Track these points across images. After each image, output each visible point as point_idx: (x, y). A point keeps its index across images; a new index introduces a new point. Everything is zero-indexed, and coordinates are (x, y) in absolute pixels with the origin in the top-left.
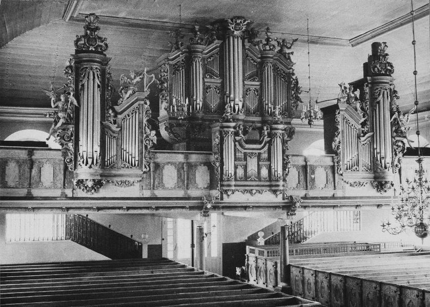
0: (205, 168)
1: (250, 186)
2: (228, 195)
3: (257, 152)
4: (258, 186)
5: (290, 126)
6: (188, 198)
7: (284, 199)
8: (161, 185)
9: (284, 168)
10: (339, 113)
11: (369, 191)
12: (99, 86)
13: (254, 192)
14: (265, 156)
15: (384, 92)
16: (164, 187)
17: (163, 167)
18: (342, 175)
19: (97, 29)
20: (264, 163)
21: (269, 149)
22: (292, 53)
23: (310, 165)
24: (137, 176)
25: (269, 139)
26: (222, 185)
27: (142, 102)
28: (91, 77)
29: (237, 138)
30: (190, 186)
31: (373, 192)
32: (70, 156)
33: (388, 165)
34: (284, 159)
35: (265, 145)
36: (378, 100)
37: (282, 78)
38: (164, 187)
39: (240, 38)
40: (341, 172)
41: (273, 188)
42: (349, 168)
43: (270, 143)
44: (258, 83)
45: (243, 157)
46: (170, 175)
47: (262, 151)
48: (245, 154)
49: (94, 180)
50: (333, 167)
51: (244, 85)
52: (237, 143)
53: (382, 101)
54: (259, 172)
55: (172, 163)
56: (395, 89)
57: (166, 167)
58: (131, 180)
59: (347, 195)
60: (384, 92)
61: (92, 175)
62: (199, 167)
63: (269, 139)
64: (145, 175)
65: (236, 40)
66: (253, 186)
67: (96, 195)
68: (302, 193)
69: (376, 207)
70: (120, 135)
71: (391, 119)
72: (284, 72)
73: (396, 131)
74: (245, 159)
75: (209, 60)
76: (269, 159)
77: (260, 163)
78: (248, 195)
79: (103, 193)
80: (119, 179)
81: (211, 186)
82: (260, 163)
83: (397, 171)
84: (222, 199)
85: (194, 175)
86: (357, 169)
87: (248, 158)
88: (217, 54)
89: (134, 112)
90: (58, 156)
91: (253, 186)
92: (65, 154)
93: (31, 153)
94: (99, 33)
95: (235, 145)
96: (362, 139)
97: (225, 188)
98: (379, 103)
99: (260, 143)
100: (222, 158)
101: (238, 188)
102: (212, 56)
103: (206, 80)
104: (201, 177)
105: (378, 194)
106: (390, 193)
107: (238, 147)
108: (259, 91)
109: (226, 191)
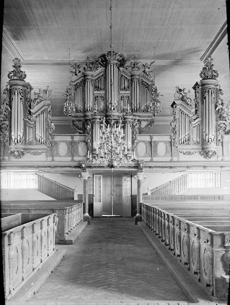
8: (58, 155)
9: (133, 143)
10: (176, 107)
11: (198, 157)
12: (21, 99)
19: (20, 67)
23: (154, 141)
24: (44, 149)
27: (47, 107)
28: (16, 94)
30: (75, 154)
31: (202, 158)
33: (210, 140)
34: (133, 137)
36: (204, 97)
40: (176, 146)
44: (129, 92)
46: (63, 148)
50: (171, 142)
51: (119, 94)
56: (221, 88)
59: (180, 160)
62: (80, 144)
68: (149, 159)
69: (203, 168)
72: (147, 84)
73: (220, 117)
80: (33, 151)
83: (221, 144)
85: (77, 148)
88: (102, 76)
96: (193, 123)
98: (205, 98)
100: (92, 138)
104: (81, 148)
105: (206, 160)
106: (214, 158)
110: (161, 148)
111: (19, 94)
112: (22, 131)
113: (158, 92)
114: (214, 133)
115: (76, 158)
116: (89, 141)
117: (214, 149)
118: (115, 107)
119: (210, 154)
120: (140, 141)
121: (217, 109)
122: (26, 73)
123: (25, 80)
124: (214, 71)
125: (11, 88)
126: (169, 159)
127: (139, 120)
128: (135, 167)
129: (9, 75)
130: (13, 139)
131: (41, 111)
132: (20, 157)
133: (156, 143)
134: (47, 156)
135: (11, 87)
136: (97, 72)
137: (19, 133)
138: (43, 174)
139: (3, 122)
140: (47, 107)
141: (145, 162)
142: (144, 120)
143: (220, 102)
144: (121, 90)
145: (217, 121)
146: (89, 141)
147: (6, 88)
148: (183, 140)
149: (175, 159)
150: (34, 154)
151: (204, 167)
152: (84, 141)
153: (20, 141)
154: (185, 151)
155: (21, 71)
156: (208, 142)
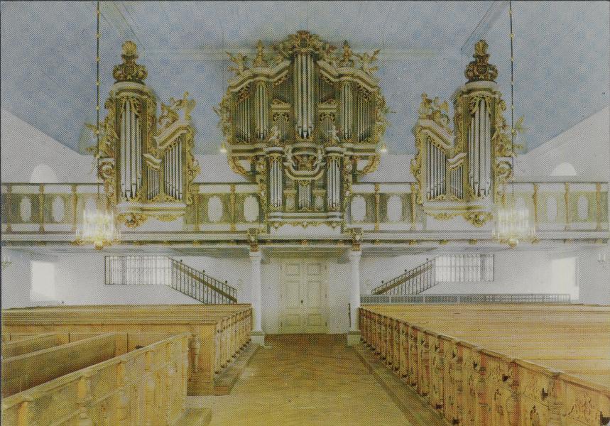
0: (255, 199)
2: (276, 228)
3: (310, 179)
4: (311, 217)
6: (234, 232)
7: (342, 232)
12: (137, 117)
13: (305, 224)
15: (480, 101)
16: (208, 221)
18: (422, 205)
19: (134, 57)
20: (319, 192)
21: (325, 177)
23: (382, 195)
24: (181, 210)
25: (323, 164)
27: (185, 131)
31: (468, 226)
33: (482, 193)
35: (319, 172)
37: (365, 98)
38: (208, 221)
39: (309, 56)
40: (421, 202)
41: (330, 219)
42: (432, 197)
43: (326, 168)
47: (316, 178)
53: (478, 112)
56: (502, 98)
57: (210, 199)
59: (428, 229)
60: (480, 101)
63: (323, 164)
65: (304, 58)
66: (305, 217)
71: (492, 136)
72: (367, 91)
74: (297, 188)
75: (277, 84)
76: (324, 187)
78: (300, 226)
81: (261, 218)
82: (314, 192)
87: (300, 187)
89: (177, 141)
91: (305, 217)
93: (74, 190)
95: (284, 173)
97: (272, 220)
98: (473, 116)
101: (286, 220)
104: (251, 209)
105: (473, 228)
107: (288, 174)
108: (336, 117)
109: (273, 223)
110: (394, 207)
112: (140, 176)
113: (387, 105)
114: (489, 180)
115: (240, 227)
116: (263, 193)
117: (487, 210)
118: (309, 132)
119: (481, 217)
120: (355, 195)
121: (495, 136)
122: (146, 69)
125: (118, 97)
127: (351, 157)
128: (345, 242)
129: (115, 72)
130: (123, 191)
131: (174, 138)
132: (137, 225)
133: (384, 198)
136: (277, 69)
137: (134, 179)
138: (182, 258)
139: (105, 160)
140: (185, 131)
141: (365, 231)
143: (501, 125)
144: (323, 101)
145: (493, 156)
146: (263, 193)
147: (109, 97)
148: (432, 192)
149: (419, 227)
150: (164, 217)
153: (136, 195)
154: (437, 212)
156: (479, 195)
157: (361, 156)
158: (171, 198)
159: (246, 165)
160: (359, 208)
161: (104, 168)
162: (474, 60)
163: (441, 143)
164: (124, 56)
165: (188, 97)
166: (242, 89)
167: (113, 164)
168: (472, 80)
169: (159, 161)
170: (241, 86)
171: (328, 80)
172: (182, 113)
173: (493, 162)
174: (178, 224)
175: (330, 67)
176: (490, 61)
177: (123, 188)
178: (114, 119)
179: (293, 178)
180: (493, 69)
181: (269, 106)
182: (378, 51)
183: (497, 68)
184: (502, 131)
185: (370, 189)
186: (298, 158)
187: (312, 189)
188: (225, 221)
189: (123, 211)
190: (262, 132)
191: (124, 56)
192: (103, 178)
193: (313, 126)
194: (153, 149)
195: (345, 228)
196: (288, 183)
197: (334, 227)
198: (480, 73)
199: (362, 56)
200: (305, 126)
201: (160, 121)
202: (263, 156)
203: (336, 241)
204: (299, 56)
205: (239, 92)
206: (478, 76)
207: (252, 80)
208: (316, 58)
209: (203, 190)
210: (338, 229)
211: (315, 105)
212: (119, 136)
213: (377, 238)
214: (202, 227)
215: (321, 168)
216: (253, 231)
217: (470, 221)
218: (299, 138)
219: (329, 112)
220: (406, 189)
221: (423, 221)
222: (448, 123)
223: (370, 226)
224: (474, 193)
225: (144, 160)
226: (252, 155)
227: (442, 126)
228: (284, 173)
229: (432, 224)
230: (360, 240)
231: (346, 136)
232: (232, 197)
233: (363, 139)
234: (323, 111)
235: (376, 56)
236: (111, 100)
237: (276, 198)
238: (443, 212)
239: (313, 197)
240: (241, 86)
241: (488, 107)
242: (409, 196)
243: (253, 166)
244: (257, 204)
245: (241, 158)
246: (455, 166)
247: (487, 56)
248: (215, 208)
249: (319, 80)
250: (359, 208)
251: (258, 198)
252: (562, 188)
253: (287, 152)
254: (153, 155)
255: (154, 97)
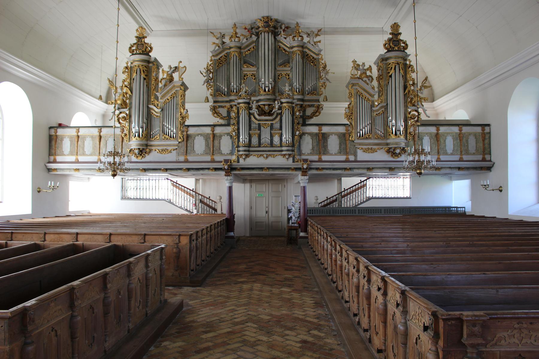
0: (229, 137)
1: (263, 151)
3: (270, 123)
5: (318, 103)
7: (294, 162)
11: (381, 155)
12: (145, 79)
14: (277, 126)
15: (395, 66)
17: (195, 138)
20: (276, 132)
22: (320, 42)
23: (324, 134)
24: (174, 145)
26: (238, 151)
29: (251, 111)
31: (387, 157)
32: (126, 132)
33: (398, 133)
36: (390, 74)
39: (270, 34)
45: (257, 127)
48: (259, 124)
49: (139, 149)
52: (252, 117)
54: (272, 140)
55: (201, 135)
56: (411, 64)
57: (197, 138)
58: (170, 148)
59: (359, 159)
60: (395, 66)
61: (137, 145)
62: (223, 137)
64: (180, 144)
65: (266, 35)
67: (143, 160)
70: (162, 115)
72: (313, 58)
74: (260, 129)
77: (272, 132)
78: (262, 158)
79: (148, 158)
82: (272, 132)
84: (238, 162)
86: (371, 136)
87: (262, 128)
90: (118, 131)
92: (123, 131)
93: (100, 131)
94: (147, 40)
95: (250, 118)
98: (391, 76)
99: (272, 115)
102: (249, 50)
103: (243, 69)
106: (403, 158)
108: (290, 75)
110: (333, 143)
111: (142, 72)
113: (327, 68)
115: (217, 158)
117: (403, 145)
121: (407, 91)
123: (150, 54)
124: (402, 40)
125: (132, 65)
126: (343, 158)
129: (130, 48)
134: (178, 155)
135: (132, 63)
139: (122, 110)
142: (310, 106)
143: (411, 83)
145: (406, 107)
146: (234, 133)
147: (126, 65)
148: (361, 132)
149: (352, 158)
151: (391, 169)
152: (228, 134)
153: (142, 135)
155: (146, 43)
156: (396, 134)
157: (309, 105)
158: (167, 137)
159: (223, 112)
160: (307, 144)
161: (121, 116)
162: (391, 36)
163: (368, 96)
164: (137, 37)
165: (182, 65)
166: (221, 57)
167: (127, 112)
168: (389, 51)
169: (160, 110)
170: (221, 55)
171: (284, 50)
172: (176, 76)
173: (406, 111)
174: (172, 156)
175: (288, 42)
176: (401, 37)
177: (134, 130)
178: (128, 80)
179: (257, 122)
180: (404, 43)
181: (241, 69)
182: (321, 30)
183: (408, 43)
184: (412, 88)
185: (314, 130)
186: (262, 106)
187: (272, 128)
188: (207, 154)
189: (133, 147)
190: (235, 88)
191: (137, 37)
192: (120, 123)
193: (273, 83)
194: (156, 102)
195: (296, 160)
196: (253, 126)
197: (288, 159)
198: (395, 46)
199: (309, 33)
200: (267, 83)
201: (161, 82)
202: (236, 105)
203: (288, 169)
204: (263, 34)
205: (219, 59)
206: (393, 48)
207: (228, 51)
208: (275, 34)
209: (191, 131)
210: (291, 159)
211: (275, 69)
212: (132, 92)
213: (320, 167)
214: (190, 158)
215: (278, 114)
216: (226, 161)
217: (390, 154)
218: (262, 92)
219: (285, 73)
220: (342, 130)
221: (355, 155)
222: (372, 81)
223: (315, 158)
224: (392, 133)
225: (149, 109)
226: (228, 105)
227: (368, 84)
228: (250, 118)
229: (362, 156)
230: (307, 168)
231: (298, 90)
232: (211, 136)
233: (311, 93)
234: (280, 72)
235: (319, 33)
236: (127, 68)
237: (243, 138)
238: (370, 147)
239: (272, 136)
240: (221, 55)
241: (401, 71)
242: (344, 135)
243: (229, 113)
244: (230, 141)
245: (220, 107)
246: (377, 113)
247: (400, 34)
248: (199, 145)
249: (277, 50)
250: (307, 144)
251: (231, 137)
252: (456, 129)
253: (253, 103)
254: (155, 106)
255: (157, 65)
